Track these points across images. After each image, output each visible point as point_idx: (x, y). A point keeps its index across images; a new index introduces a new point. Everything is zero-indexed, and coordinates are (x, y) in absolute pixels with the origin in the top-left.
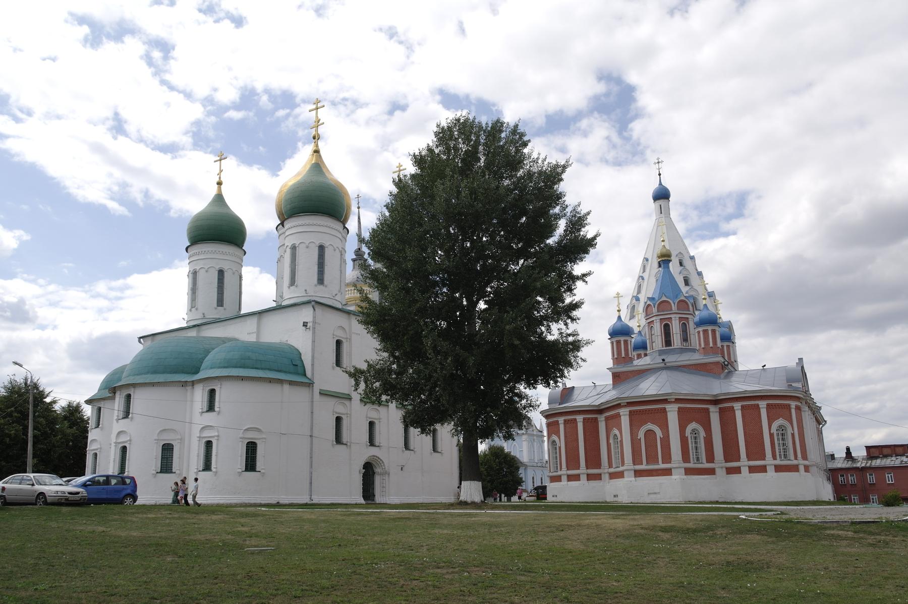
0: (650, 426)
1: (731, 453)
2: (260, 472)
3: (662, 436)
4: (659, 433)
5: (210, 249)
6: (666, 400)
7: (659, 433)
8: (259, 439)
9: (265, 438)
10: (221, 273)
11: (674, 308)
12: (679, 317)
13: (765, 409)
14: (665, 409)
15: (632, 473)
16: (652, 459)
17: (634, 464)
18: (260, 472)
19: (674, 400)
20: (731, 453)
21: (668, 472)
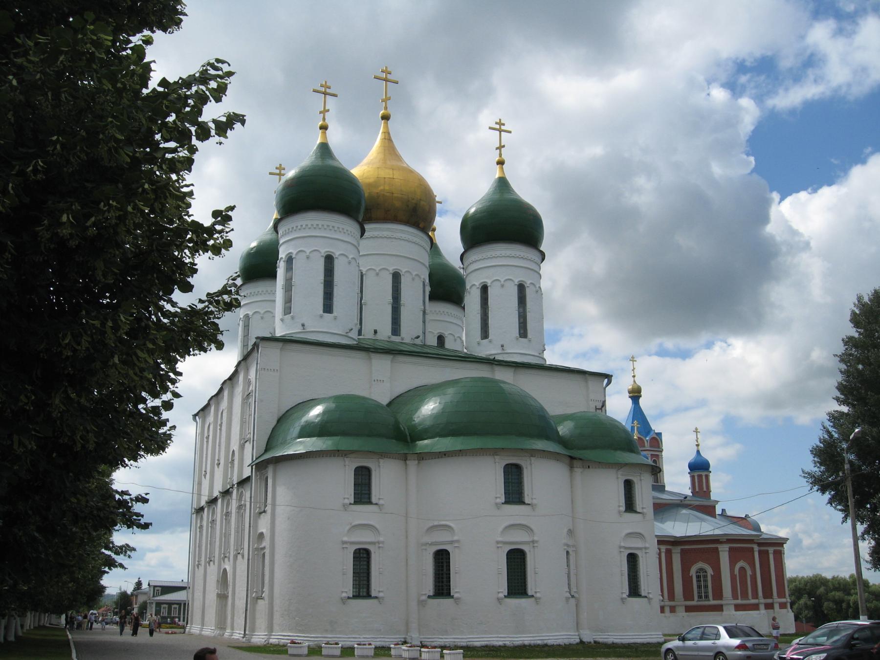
0: (700, 565)
1: (768, 594)
2: (646, 597)
3: (712, 574)
4: (710, 572)
5: (320, 223)
6: (718, 540)
7: (710, 572)
8: (640, 549)
9: (646, 548)
10: (329, 260)
11: (647, 445)
12: (651, 455)
13: (727, 553)
14: (717, 548)
15: (732, 607)
16: (745, 595)
17: (685, 600)
18: (646, 597)
19: (725, 540)
20: (768, 594)
21: (719, 608)
